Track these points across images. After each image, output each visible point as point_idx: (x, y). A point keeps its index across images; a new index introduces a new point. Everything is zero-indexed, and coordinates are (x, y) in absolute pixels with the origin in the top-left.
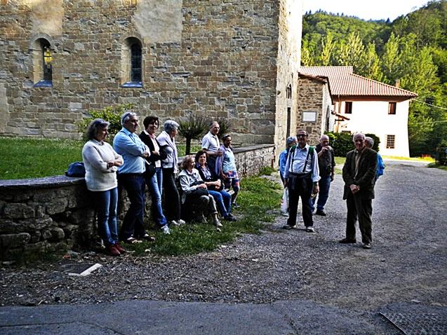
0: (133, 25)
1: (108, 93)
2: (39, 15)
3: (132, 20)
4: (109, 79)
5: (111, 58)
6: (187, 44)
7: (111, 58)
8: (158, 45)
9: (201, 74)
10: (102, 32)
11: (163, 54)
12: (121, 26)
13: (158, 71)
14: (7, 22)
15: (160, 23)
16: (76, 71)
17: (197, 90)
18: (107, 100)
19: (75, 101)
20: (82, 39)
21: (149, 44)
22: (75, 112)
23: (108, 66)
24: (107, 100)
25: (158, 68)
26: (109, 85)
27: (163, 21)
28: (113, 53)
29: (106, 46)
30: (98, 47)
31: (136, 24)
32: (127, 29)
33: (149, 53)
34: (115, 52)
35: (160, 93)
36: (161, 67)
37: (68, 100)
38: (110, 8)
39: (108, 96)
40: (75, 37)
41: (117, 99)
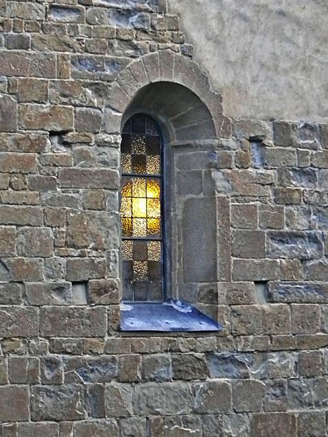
0: (175, 25)
1: (52, 364)
4: (60, 289)
5: (74, 178)
7: (74, 178)
8: (282, 130)
10: (23, 44)
11: (302, 172)
12: (114, 24)
13: (283, 253)
15: (288, 30)
18: (46, 402)
21: (243, 125)
23: (56, 219)
24: (46, 402)
25: (282, 238)
26: (59, 320)
27: (298, 22)
28: (83, 156)
31: (187, 22)
32: (144, 41)
33: (243, 164)
34: (91, 150)
35: (292, 358)
36: (295, 236)
39: (56, 381)
41: (96, 400)
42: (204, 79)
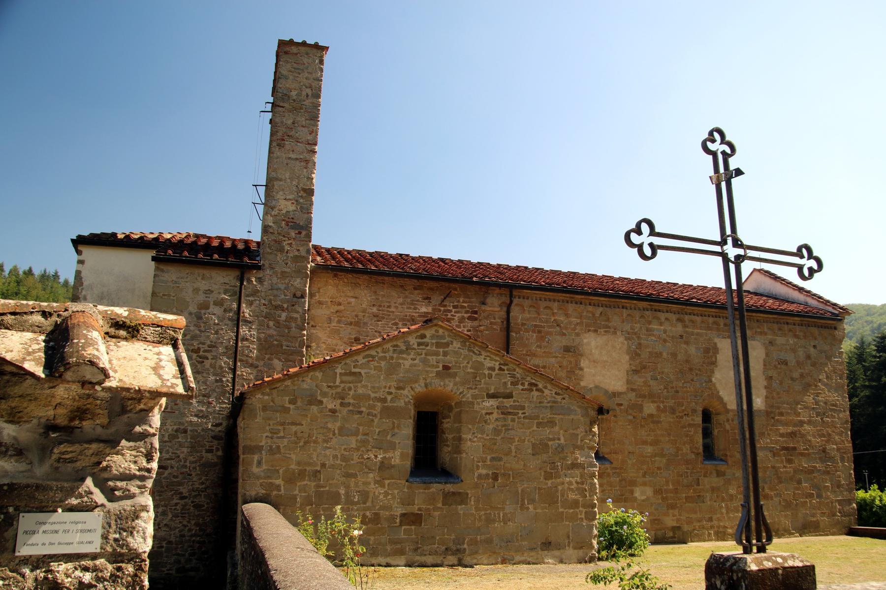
2: (594, 361)
3: (713, 379)
6: (771, 412)
9: (787, 449)
14: (544, 367)
16: (645, 443)
17: (785, 467)
19: (644, 484)
20: (652, 397)
22: (643, 501)
23: (687, 436)
29: (683, 411)
30: (673, 411)
37: (633, 483)
38: (687, 361)
40: (644, 396)
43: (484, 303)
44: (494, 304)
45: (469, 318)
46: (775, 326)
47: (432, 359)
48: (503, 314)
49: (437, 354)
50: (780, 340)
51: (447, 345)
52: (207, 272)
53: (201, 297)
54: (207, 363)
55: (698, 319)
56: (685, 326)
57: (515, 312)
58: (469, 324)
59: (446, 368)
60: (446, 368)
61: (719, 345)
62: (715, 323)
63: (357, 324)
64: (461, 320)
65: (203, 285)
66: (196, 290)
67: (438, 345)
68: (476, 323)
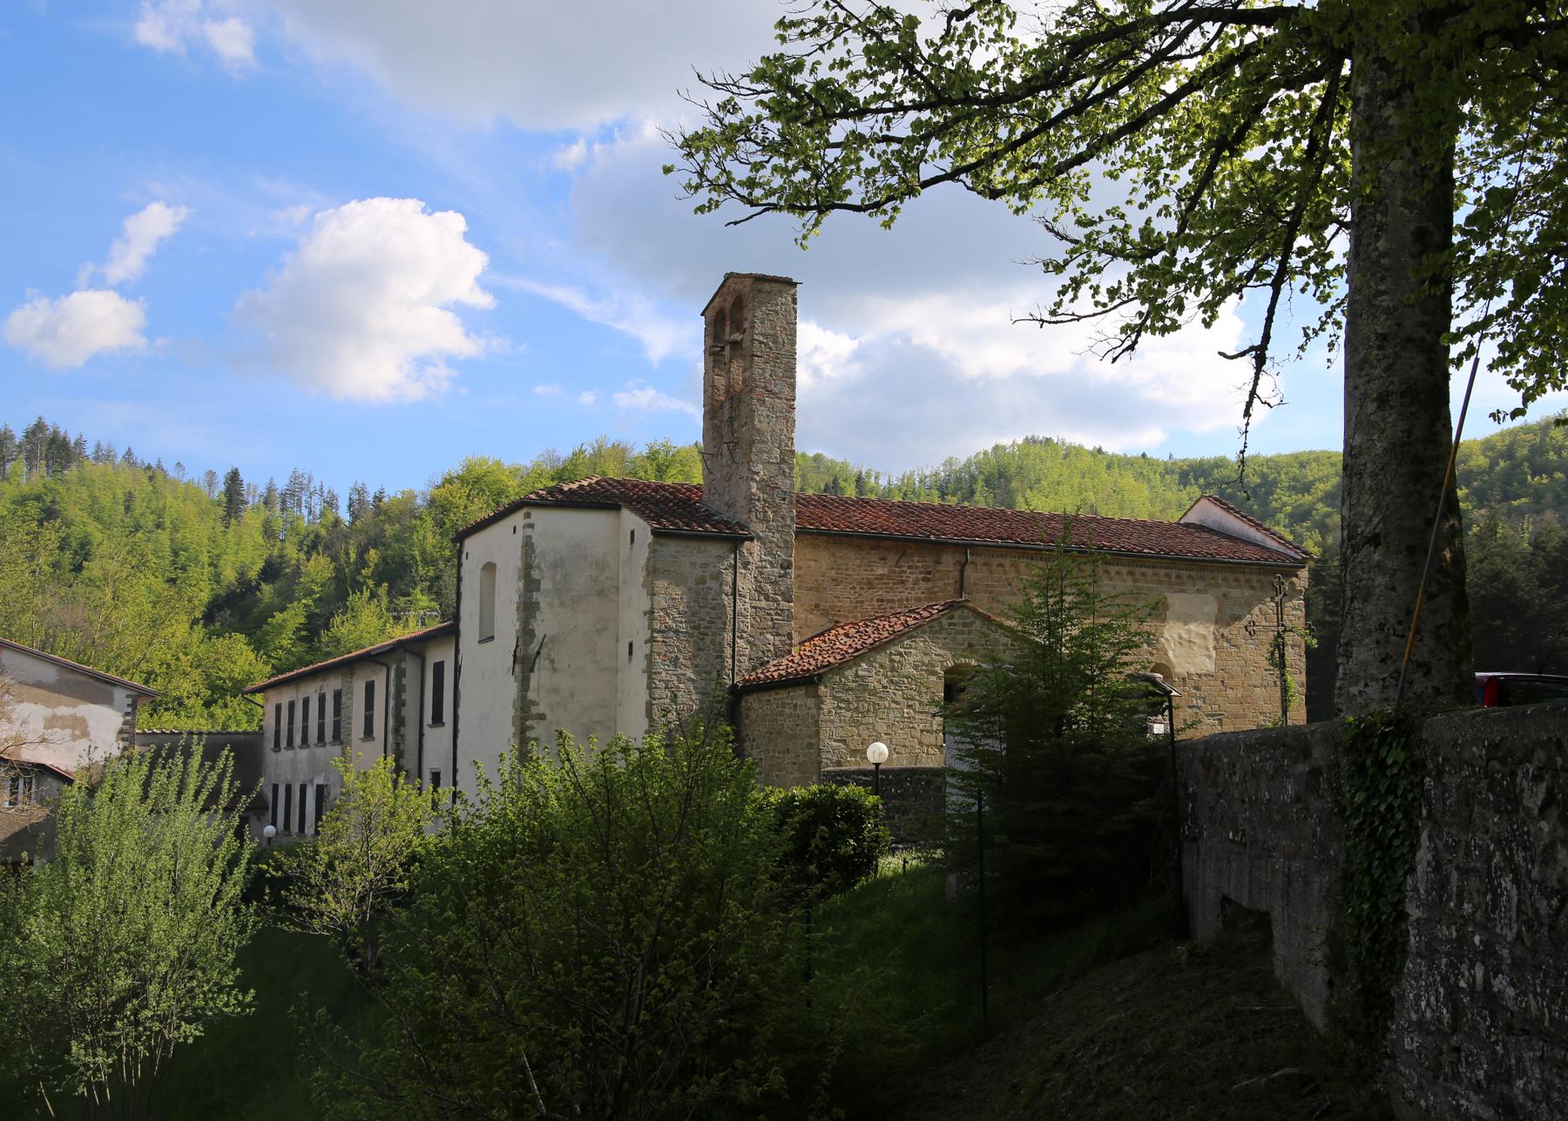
42: (1169, 661)
43: (938, 563)
44: (949, 561)
45: (924, 579)
46: (1231, 577)
47: (959, 637)
48: (957, 573)
49: (963, 633)
50: (1235, 593)
51: (971, 624)
52: (703, 546)
53: (699, 572)
54: (708, 640)
55: (1149, 572)
56: (1135, 581)
57: (969, 572)
58: (923, 585)
59: (970, 645)
60: (970, 645)
61: (1170, 601)
62: (1167, 575)
63: (817, 589)
64: (916, 582)
65: (699, 559)
66: (693, 564)
67: (965, 625)
68: (930, 584)
